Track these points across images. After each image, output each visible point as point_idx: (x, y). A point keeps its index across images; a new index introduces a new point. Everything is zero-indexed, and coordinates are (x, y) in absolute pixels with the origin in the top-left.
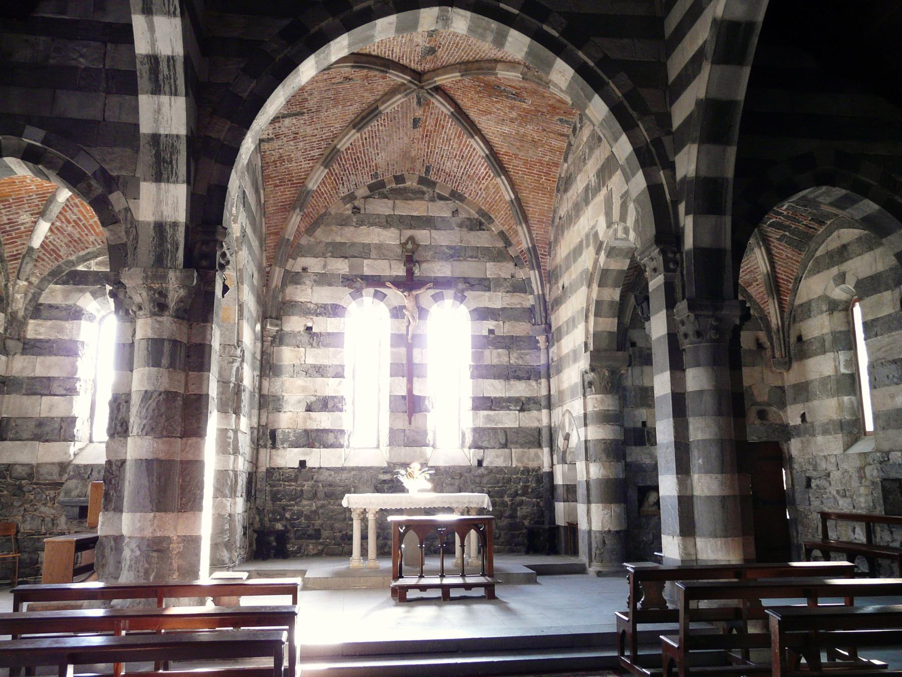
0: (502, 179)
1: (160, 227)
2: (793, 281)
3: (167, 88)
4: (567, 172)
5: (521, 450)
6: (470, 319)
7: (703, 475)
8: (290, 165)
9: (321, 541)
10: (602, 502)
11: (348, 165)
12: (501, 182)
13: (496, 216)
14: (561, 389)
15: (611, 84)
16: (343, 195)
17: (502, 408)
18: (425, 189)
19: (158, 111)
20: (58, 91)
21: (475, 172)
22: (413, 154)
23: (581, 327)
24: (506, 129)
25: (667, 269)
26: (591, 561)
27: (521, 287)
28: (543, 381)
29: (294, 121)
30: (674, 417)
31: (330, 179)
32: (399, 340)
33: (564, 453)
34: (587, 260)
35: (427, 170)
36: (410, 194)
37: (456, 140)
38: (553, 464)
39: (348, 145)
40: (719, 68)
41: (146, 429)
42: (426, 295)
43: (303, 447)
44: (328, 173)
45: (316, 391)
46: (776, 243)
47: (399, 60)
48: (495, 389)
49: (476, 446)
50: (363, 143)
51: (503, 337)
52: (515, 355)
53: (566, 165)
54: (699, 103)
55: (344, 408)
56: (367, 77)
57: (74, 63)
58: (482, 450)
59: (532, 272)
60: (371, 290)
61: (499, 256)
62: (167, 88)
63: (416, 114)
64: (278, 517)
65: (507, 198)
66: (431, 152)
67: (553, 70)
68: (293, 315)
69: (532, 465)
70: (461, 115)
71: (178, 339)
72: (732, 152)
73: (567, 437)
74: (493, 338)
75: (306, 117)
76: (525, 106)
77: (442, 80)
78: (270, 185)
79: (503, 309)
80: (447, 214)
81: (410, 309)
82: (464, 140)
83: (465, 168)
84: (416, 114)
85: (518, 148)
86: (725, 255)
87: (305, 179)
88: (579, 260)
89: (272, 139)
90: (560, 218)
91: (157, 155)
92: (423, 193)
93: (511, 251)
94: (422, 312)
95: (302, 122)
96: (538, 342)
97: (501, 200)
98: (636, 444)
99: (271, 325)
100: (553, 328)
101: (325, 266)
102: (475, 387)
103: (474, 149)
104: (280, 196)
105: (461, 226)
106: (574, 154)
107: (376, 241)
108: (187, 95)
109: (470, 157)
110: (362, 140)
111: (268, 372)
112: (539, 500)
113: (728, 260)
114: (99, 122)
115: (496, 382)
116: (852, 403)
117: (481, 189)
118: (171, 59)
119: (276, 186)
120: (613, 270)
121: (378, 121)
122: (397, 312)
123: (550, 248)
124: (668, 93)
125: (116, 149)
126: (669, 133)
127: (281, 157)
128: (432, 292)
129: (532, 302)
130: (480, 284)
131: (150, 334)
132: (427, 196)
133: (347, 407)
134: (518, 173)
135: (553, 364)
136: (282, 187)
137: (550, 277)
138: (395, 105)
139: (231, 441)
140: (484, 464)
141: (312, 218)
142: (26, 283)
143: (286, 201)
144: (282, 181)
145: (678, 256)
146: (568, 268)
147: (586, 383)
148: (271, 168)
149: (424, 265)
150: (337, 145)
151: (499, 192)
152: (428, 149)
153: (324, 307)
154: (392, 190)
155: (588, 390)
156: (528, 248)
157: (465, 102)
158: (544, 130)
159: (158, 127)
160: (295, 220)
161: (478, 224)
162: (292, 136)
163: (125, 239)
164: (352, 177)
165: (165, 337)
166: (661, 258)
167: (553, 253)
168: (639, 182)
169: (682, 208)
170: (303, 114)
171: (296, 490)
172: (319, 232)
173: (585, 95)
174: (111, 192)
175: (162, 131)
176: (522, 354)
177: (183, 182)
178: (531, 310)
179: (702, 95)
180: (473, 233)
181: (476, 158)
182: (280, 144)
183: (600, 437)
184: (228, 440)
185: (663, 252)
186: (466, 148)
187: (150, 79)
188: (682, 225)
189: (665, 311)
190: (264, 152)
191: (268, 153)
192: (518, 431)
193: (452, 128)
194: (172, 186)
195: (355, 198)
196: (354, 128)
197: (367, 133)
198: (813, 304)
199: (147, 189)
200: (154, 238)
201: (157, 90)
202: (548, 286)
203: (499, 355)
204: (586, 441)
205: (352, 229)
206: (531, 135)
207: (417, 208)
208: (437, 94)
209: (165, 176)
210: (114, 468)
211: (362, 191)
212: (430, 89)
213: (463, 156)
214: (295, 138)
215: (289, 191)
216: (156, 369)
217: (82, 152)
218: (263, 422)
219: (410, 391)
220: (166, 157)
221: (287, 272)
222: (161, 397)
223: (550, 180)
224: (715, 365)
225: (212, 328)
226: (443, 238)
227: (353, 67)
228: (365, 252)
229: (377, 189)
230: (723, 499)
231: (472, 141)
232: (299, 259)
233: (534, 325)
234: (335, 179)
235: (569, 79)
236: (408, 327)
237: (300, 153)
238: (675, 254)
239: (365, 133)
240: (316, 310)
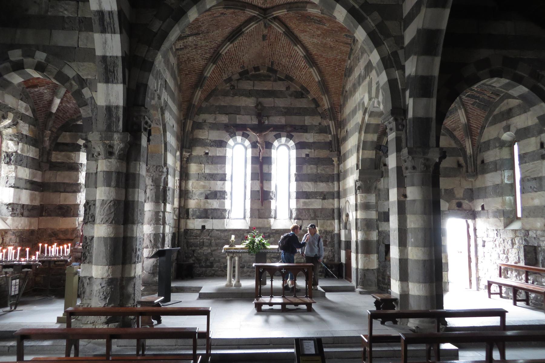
0: (313, 69)
1: (109, 109)
2: (480, 128)
3: (109, 30)
4: (350, 65)
5: (322, 221)
6: (295, 148)
7: (413, 248)
8: (194, 63)
9: (213, 268)
10: (364, 254)
11: (227, 62)
12: (313, 71)
13: (311, 90)
14: (345, 188)
15: (369, 19)
16: (225, 78)
17: (313, 198)
18: (271, 74)
19: (105, 43)
20: (53, 31)
21: (298, 65)
22: (264, 54)
23: (355, 155)
24: (315, 41)
25: (398, 129)
26: (357, 285)
27: (324, 130)
28: (336, 183)
29: (195, 38)
30: (398, 214)
31: (217, 70)
32: (255, 160)
33: (346, 223)
34: (358, 118)
35: (272, 63)
36: (263, 78)
37: (287, 47)
38: (340, 229)
39: (226, 50)
40: (429, 10)
41: (103, 220)
42: (271, 135)
43: (204, 218)
44: (215, 66)
45: (210, 188)
46: (471, 106)
47: (251, 3)
48: (309, 187)
49: (297, 218)
50: (235, 50)
51: (314, 158)
52: (320, 168)
53: (349, 61)
54: (419, 31)
55: (226, 197)
56: (234, 13)
57: (61, 14)
58: (301, 221)
59: (330, 122)
60: (241, 133)
61: (313, 112)
62: (109, 30)
63: (264, 33)
64: (190, 256)
65: (317, 80)
66: (274, 54)
67: (335, 10)
68: (198, 146)
69: (328, 229)
70: (289, 33)
72: (437, 60)
73: (347, 215)
74: (308, 159)
75: (201, 36)
76: (325, 27)
77: (276, 13)
78: (183, 74)
79: (314, 143)
80: (284, 89)
81: (261, 143)
82: (292, 47)
83: (293, 63)
84: (264, 33)
85: (322, 52)
86: (432, 121)
87: (203, 70)
88: (355, 117)
89: (183, 49)
90: (346, 91)
91: (106, 68)
92: (270, 77)
93: (319, 110)
94: (269, 146)
95: (199, 38)
96: (333, 161)
97: (314, 81)
98: (384, 221)
99: (186, 152)
100: (342, 154)
101: (215, 119)
102: (298, 186)
103: (298, 52)
104: (189, 80)
105: (291, 95)
106: (354, 55)
107: (243, 105)
108: (121, 33)
109: (296, 57)
110: (234, 48)
111: (184, 178)
112: (332, 248)
113: (434, 124)
114: (76, 48)
115: (310, 184)
116: (510, 200)
117: (302, 74)
118: (111, 13)
119: (186, 74)
120: (373, 124)
121: (242, 37)
122: (254, 145)
123: (341, 108)
124: (402, 24)
125: (86, 64)
126: (402, 48)
127: (189, 58)
128: (275, 133)
129: (330, 139)
130: (301, 129)
131: (105, 169)
132: (272, 79)
133: (228, 196)
134: (323, 66)
135: (341, 174)
136: (190, 75)
137: (341, 124)
138: (252, 28)
139: (161, 218)
140: (302, 229)
141: (208, 92)
142: (50, 132)
143: (192, 83)
144: (189, 72)
145: (404, 121)
146: (349, 121)
147: (357, 187)
149: (271, 118)
150: (220, 51)
151: (312, 76)
152: (272, 52)
153: (215, 141)
154: (253, 76)
155: (358, 191)
156: (328, 108)
157: (291, 25)
158: (337, 41)
159: (105, 52)
160: (199, 95)
161: (302, 93)
163: (91, 115)
164: (230, 69)
165: (112, 170)
166: (394, 123)
167: (342, 111)
168: (384, 78)
169: (407, 93)
170: (199, 34)
171: (200, 241)
172: (211, 100)
173: (353, 25)
174: (83, 88)
175: (108, 54)
176: (325, 167)
177: (121, 83)
178: (330, 143)
179: (420, 27)
180: (298, 99)
181: (299, 57)
182: (188, 51)
183: (363, 218)
184: (160, 217)
185: (396, 120)
186: (293, 52)
187: (100, 24)
188: (407, 103)
189: (395, 154)
190: (179, 56)
192: (322, 210)
193: (284, 40)
194: (115, 85)
195: (232, 80)
196: (229, 41)
197: (237, 44)
198: (491, 142)
199: (101, 87)
200: (106, 115)
201: (104, 31)
202: (339, 130)
203: (311, 168)
204: (356, 219)
205: (230, 98)
206: (330, 44)
207: (266, 86)
208: (275, 21)
209: (111, 80)
210: (88, 241)
211: (236, 77)
212: (270, 19)
213: (291, 56)
214: (196, 48)
215: (194, 77)
216: (108, 188)
217: (67, 65)
218: (182, 205)
219: (262, 188)
221: (194, 122)
223: (341, 70)
224: (422, 186)
225: (140, 164)
226: (280, 103)
227: (224, 8)
228: (237, 111)
229: (244, 75)
230: (424, 261)
231: (296, 48)
232: (201, 115)
233: (331, 151)
234: (220, 70)
235: (344, 16)
236: (260, 152)
237: (199, 56)
238: (403, 120)
239: (235, 44)
240: (210, 143)
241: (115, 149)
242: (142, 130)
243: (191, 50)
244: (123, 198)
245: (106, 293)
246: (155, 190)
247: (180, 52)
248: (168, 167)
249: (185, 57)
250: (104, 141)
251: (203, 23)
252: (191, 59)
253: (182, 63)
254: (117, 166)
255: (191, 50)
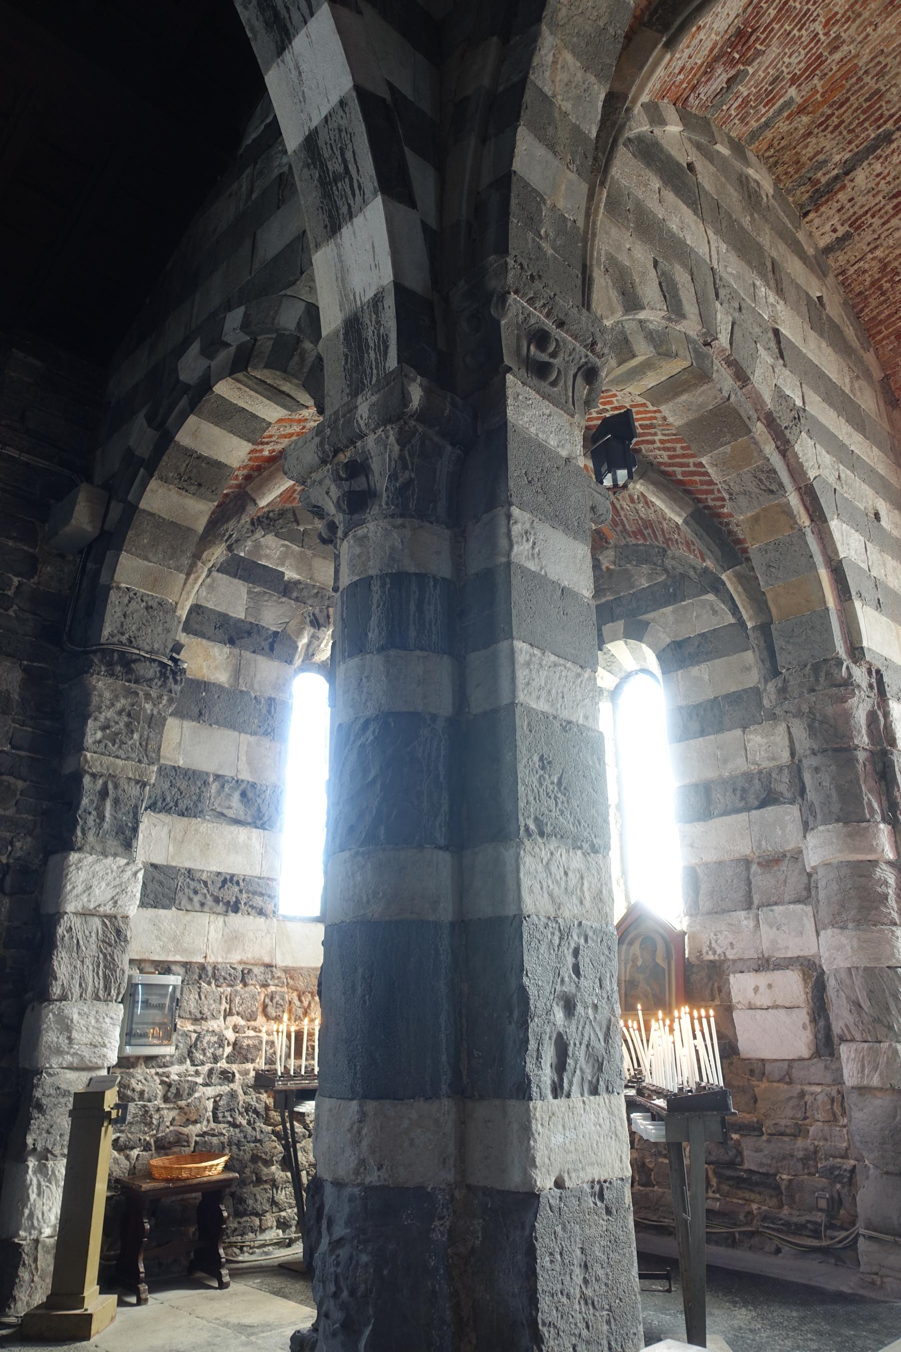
71: (412, 569)
78: (887, 337)
89: (847, 236)
127: (886, 266)
148: (873, 303)
162: (889, 207)
165: (372, 572)
182: (869, 238)
184: (879, 890)
190: (843, 272)
191: (852, 270)
200: (346, 356)
220: (337, 166)
222: (371, 729)
225: (509, 516)
241: (377, 474)
242: (508, 361)
243: (884, 224)
244: (444, 706)
245: (353, 1293)
246: (833, 767)
247: (841, 258)
248: (877, 664)
249: (867, 266)
250: (335, 461)
251: (881, 74)
252: (896, 264)
253: (866, 298)
254: (393, 548)
255: (884, 224)
